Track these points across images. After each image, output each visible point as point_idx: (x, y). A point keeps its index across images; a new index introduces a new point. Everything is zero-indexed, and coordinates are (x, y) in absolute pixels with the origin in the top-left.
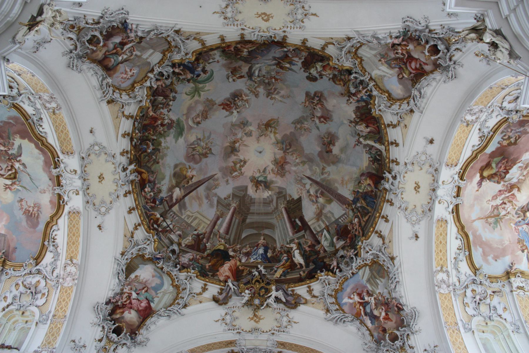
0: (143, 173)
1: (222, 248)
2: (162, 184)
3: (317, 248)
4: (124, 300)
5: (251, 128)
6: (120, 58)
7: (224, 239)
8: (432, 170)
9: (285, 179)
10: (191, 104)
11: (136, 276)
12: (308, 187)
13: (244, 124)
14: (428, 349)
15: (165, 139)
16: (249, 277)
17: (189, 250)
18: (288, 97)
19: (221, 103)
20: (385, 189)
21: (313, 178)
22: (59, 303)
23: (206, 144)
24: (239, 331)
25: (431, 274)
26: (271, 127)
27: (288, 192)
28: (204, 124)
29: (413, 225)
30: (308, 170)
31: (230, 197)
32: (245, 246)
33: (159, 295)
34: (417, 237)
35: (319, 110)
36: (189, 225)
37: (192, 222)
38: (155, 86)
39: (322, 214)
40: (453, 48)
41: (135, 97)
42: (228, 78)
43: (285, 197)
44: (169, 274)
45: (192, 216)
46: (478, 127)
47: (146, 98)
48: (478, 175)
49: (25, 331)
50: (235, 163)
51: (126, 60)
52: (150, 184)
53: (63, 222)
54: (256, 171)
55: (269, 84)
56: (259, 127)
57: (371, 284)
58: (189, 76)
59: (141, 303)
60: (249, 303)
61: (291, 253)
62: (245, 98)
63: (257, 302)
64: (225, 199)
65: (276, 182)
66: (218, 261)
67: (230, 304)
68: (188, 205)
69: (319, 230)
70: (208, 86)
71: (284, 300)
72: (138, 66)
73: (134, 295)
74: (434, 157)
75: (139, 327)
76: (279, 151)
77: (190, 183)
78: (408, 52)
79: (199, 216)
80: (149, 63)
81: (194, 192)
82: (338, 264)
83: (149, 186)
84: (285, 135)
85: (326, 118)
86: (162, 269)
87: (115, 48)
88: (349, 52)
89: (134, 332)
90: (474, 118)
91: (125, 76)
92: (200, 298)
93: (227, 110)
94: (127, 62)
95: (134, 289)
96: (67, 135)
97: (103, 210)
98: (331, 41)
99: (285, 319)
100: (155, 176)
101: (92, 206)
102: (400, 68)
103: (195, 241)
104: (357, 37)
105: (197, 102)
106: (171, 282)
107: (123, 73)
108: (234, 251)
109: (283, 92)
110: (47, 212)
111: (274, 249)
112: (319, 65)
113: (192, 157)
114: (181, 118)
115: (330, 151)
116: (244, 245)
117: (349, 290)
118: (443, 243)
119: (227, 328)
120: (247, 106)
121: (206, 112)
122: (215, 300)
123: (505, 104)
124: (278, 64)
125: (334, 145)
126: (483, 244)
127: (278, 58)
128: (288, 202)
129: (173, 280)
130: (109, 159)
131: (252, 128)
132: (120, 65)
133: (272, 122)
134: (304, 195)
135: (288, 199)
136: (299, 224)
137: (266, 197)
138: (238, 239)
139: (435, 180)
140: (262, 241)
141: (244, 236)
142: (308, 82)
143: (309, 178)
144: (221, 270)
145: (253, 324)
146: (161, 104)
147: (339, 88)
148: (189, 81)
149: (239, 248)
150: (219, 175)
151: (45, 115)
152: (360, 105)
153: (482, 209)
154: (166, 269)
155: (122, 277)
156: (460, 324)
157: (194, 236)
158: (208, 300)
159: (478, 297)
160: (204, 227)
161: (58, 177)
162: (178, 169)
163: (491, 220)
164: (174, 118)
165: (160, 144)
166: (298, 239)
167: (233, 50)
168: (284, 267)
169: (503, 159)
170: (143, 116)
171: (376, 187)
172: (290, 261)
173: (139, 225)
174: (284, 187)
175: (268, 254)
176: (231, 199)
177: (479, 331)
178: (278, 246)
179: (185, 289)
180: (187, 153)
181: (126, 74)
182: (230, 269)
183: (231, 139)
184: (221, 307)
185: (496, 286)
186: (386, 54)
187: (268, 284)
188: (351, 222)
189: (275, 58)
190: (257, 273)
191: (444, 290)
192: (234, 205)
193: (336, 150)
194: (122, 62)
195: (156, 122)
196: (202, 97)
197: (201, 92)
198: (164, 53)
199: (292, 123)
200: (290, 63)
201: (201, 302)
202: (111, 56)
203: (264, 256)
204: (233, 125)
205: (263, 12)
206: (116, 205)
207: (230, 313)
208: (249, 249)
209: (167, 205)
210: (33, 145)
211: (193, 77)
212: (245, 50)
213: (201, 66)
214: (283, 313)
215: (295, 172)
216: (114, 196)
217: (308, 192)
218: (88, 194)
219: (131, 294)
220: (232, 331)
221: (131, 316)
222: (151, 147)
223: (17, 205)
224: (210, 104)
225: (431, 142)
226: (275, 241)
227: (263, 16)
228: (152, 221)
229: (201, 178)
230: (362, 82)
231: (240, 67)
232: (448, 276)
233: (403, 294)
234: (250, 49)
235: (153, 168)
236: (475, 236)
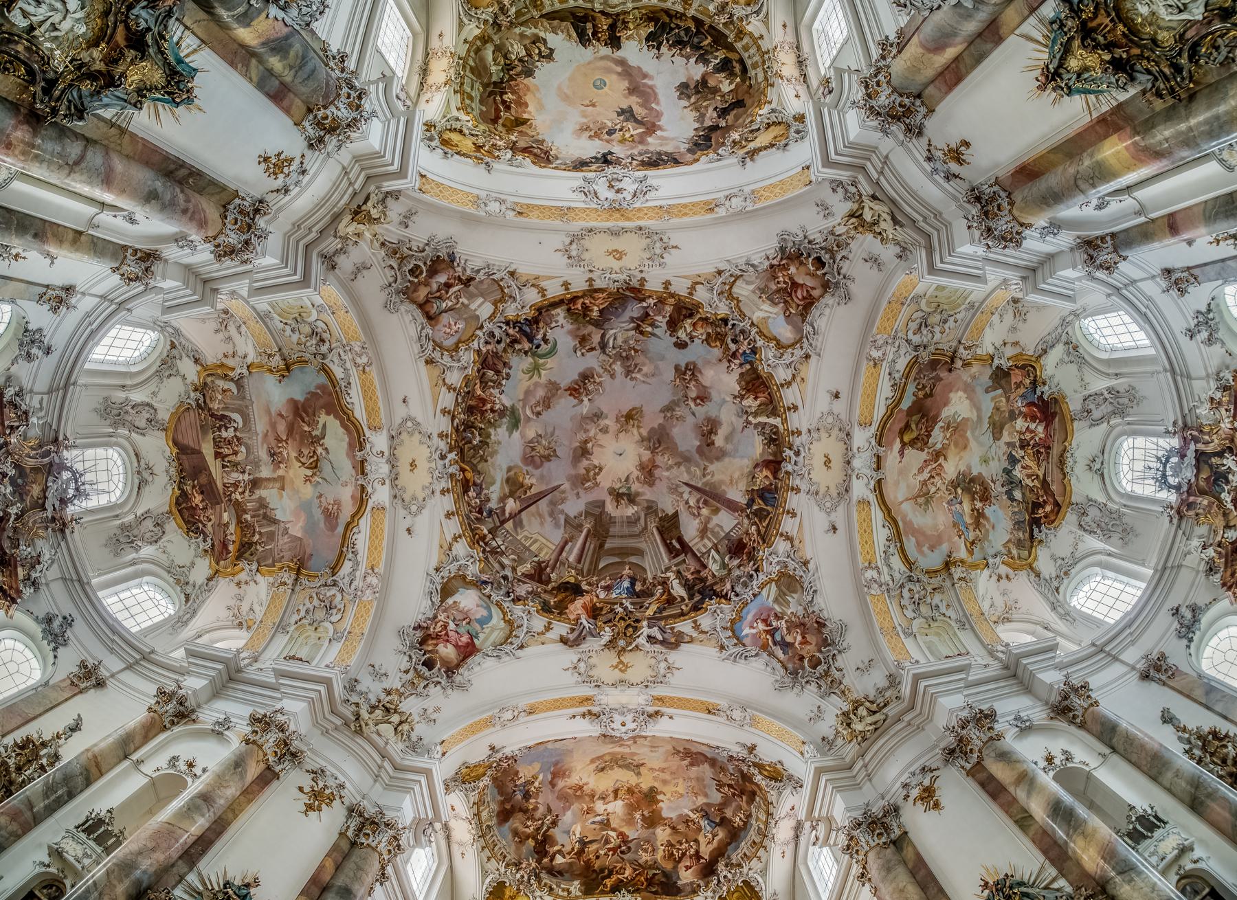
1: (572, 580)
3: (704, 574)
4: (438, 629)
5: (607, 422)
7: (575, 569)
8: (843, 435)
9: (655, 488)
12: (686, 496)
13: (597, 416)
14: (861, 666)
16: (610, 616)
20: (787, 473)
22: (356, 618)
25: (856, 573)
27: (660, 506)
28: (546, 415)
29: (828, 513)
34: (834, 529)
36: (528, 549)
38: (484, 350)
40: (839, 257)
41: (459, 361)
43: (656, 512)
44: (499, 605)
46: (888, 371)
48: (898, 440)
49: (317, 647)
50: (588, 470)
51: (450, 309)
53: (365, 523)
55: (627, 358)
56: (617, 420)
57: (780, 604)
58: (527, 346)
60: (611, 644)
62: (598, 380)
63: (622, 643)
65: (643, 494)
67: (584, 647)
68: (525, 522)
70: (550, 362)
71: (660, 638)
74: (843, 417)
75: (458, 666)
78: (791, 279)
79: (540, 538)
80: (478, 317)
82: (733, 587)
84: (652, 429)
85: (703, 398)
86: (489, 597)
87: (439, 290)
88: (722, 293)
89: (451, 670)
90: (880, 354)
92: (542, 638)
96: (376, 402)
97: (414, 508)
98: (699, 280)
99: (663, 665)
102: (785, 302)
104: (728, 268)
105: (536, 385)
108: (589, 584)
109: (645, 369)
110: (348, 509)
111: (645, 580)
112: (688, 323)
115: (711, 444)
117: (750, 617)
118: (868, 531)
119: (580, 679)
121: (549, 398)
122: (564, 641)
123: (911, 336)
124: (637, 328)
125: (716, 434)
126: (917, 532)
128: (661, 519)
129: (504, 614)
130: (426, 440)
131: (609, 422)
134: (682, 508)
136: (678, 546)
138: (593, 570)
139: (848, 449)
140: (626, 571)
142: (676, 350)
143: (687, 484)
144: (571, 607)
145: (617, 674)
147: (717, 352)
148: (526, 353)
150: (567, 486)
151: (354, 372)
152: (744, 370)
153: (908, 486)
154: (495, 597)
155: (437, 599)
156: (899, 628)
158: (554, 641)
159: (917, 596)
161: (362, 462)
162: (512, 473)
163: (921, 500)
164: (508, 404)
165: (489, 436)
166: (676, 565)
169: (922, 417)
170: (468, 393)
171: (775, 478)
173: (460, 536)
177: (921, 634)
178: (650, 576)
179: (520, 626)
180: (525, 454)
182: (584, 607)
183: (582, 436)
184: (571, 650)
185: (936, 582)
186: (766, 286)
187: (638, 621)
188: (747, 533)
189: (632, 320)
190: (621, 610)
191: (875, 590)
192: (587, 526)
193: (719, 440)
194: (446, 312)
198: (495, 304)
199: (661, 411)
200: (652, 325)
204: (585, 418)
206: (430, 503)
210: (338, 422)
212: (596, 308)
213: (542, 332)
214: (660, 657)
215: (668, 478)
216: (428, 492)
217: (687, 502)
221: (447, 651)
222: (478, 438)
223: (316, 501)
224: (553, 387)
225: (837, 396)
226: (644, 570)
229: (543, 488)
230: (742, 332)
231: (589, 335)
232: (879, 573)
233: (823, 606)
235: (479, 467)
236: (905, 523)
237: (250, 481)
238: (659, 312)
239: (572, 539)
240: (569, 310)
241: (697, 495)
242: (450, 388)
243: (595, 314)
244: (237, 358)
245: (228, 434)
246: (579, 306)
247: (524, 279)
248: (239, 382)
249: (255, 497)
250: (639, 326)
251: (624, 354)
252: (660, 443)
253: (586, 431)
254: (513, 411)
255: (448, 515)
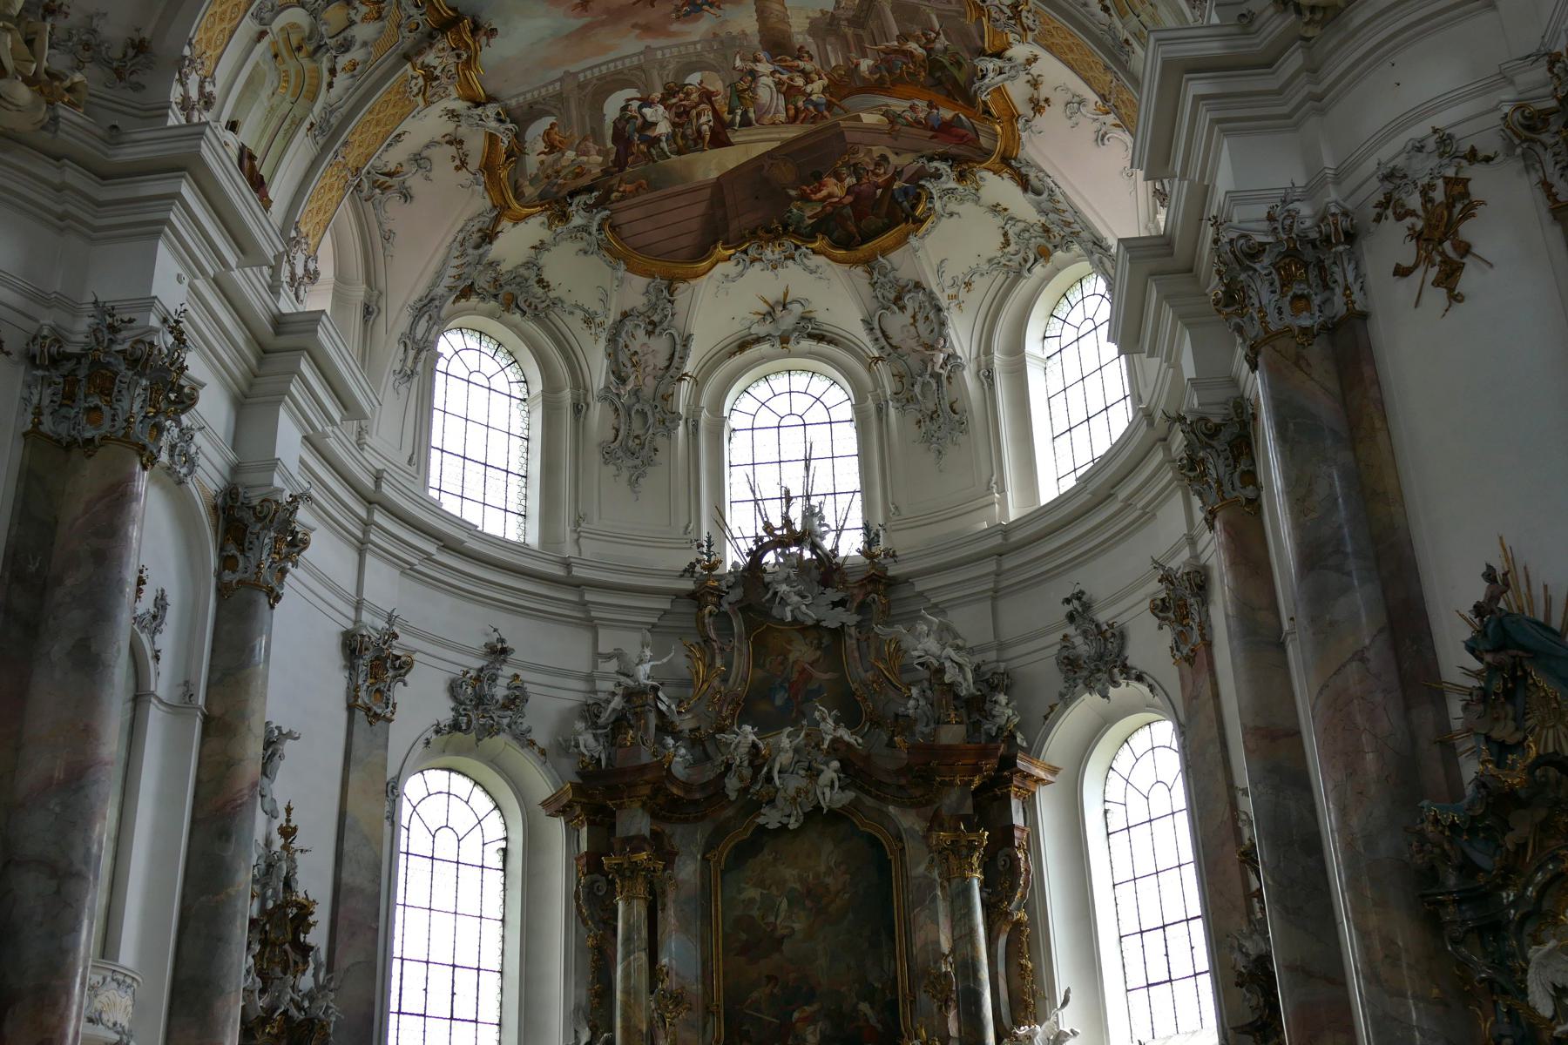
237: (773, 59)
244: (464, 130)
245: (661, 120)
248: (520, 118)
249: (811, 46)
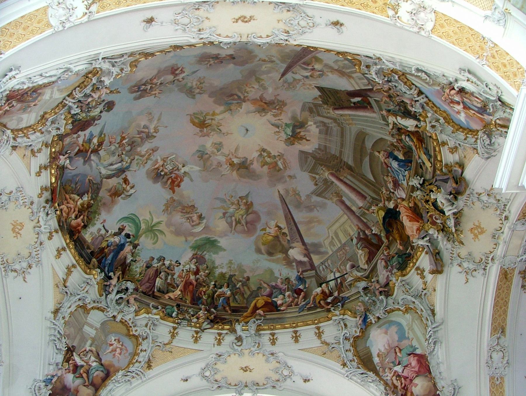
0: (256, 304)
1: (382, 214)
2: (279, 277)
6: (94, 364)
7: (371, 204)
10: (172, 232)
11: (378, 355)
12: (298, 77)
15: (217, 267)
17: (374, 262)
18: (151, 114)
19: (171, 191)
21: (282, 70)
23: (233, 204)
24: (491, 257)
26: (205, 121)
27: (310, 100)
28: (202, 209)
30: (270, 75)
31: (315, 178)
32: (385, 181)
33: (411, 336)
35: (162, 79)
37: (340, 241)
39: (340, 70)
42: (131, 195)
43: (316, 105)
45: (332, 238)
47: (150, 315)
50: (264, 164)
51: (98, 356)
52: (273, 296)
54: (277, 137)
56: (208, 135)
58: (128, 248)
59: (411, 364)
61: (401, 129)
62: (161, 163)
64: (316, 185)
66: (398, 229)
68: (315, 240)
69: (365, 81)
70: (144, 216)
72: (106, 336)
73: (399, 369)
75: (435, 385)
76: (243, 107)
77: (286, 231)
80: (103, 324)
81: (300, 227)
83: (276, 297)
84: (215, 102)
86: (379, 318)
87: (81, 376)
91: (118, 350)
93: (182, 180)
94: (99, 353)
95: (392, 365)
97: (286, 373)
100: (265, 285)
101: (278, 383)
103: (366, 247)
105: (169, 224)
106: (401, 313)
107: (114, 355)
108: (389, 199)
113: (249, 225)
114: (191, 244)
116: (383, 183)
120: (174, 156)
121: (184, 208)
122: (438, 270)
124: (95, 151)
125: (219, 54)
127: (84, 159)
128: (325, 102)
129: (399, 310)
132: (103, 362)
133: (196, 121)
135: (321, 103)
137: (318, 130)
141: (372, 178)
143: (283, 75)
146: (166, 279)
148: (135, 246)
149: (386, 190)
150: (281, 187)
157: (359, 246)
158: (435, 280)
160: (350, 226)
162: (263, 248)
164: (189, 254)
165: (223, 275)
166: (381, 109)
167: (82, 217)
168: (419, 148)
170: (178, 306)
172: (412, 137)
174: (301, 104)
175: (400, 157)
176: (317, 177)
178: (389, 138)
180: (244, 232)
181: (116, 351)
183: (225, 169)
189: (87, 160)
192: (326, 174)
194: (100, 360)
195: (191, 283)
196: (161, 220)
197: (153, 224)
199: (193, 97)
200: (90, 141)
201: (435, 290)
202: (91, 377)
203: (402, 164)
204: (205, 168)
205: (12, 232)
207: (459, 261)
208: (390, 179)
209: (309, 272)
211: (131, 242)
213: (112, 240)
215: (277, 88)
216: (271, 358)
217: (307, 77)
218: (264, 384)
219: (395, 372)
220: (489, 266)
226: (381, 139)
227: (17, 230)
228: (322, 302)
229: (281, 213)
234: (76, 197)
235: (254, 288)
238: (75, 143)
239: (339, 195)
240: (85, 227)
241: (296, 68)
242: (173, 336)
243: (86, 198)
246: (79, 220)
247: (59, 296)
250: (92, 152)
251: (128, 148)
252: (232, 95)
253: (220, 164)
254: (197, 247)
255: (296, 338)
